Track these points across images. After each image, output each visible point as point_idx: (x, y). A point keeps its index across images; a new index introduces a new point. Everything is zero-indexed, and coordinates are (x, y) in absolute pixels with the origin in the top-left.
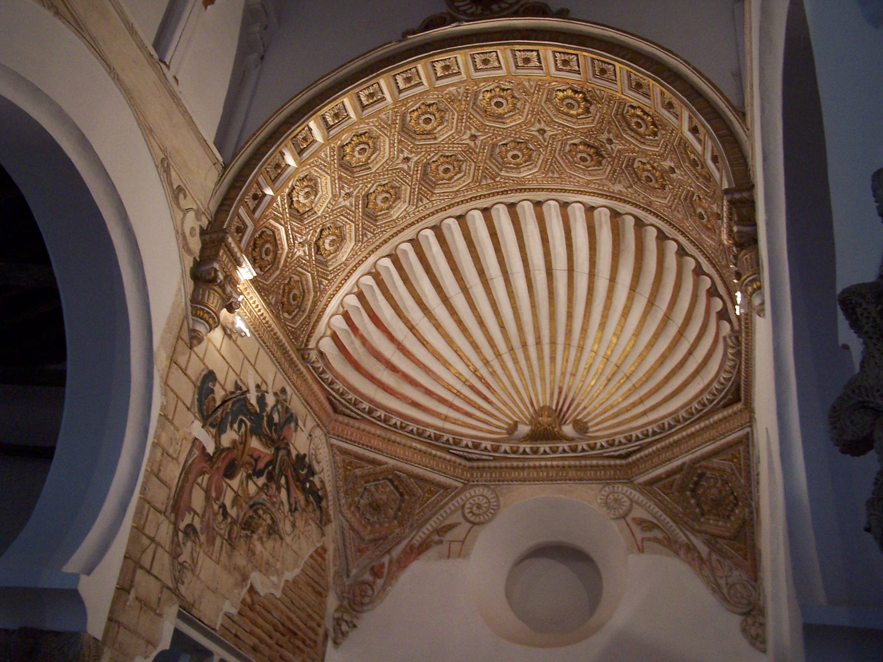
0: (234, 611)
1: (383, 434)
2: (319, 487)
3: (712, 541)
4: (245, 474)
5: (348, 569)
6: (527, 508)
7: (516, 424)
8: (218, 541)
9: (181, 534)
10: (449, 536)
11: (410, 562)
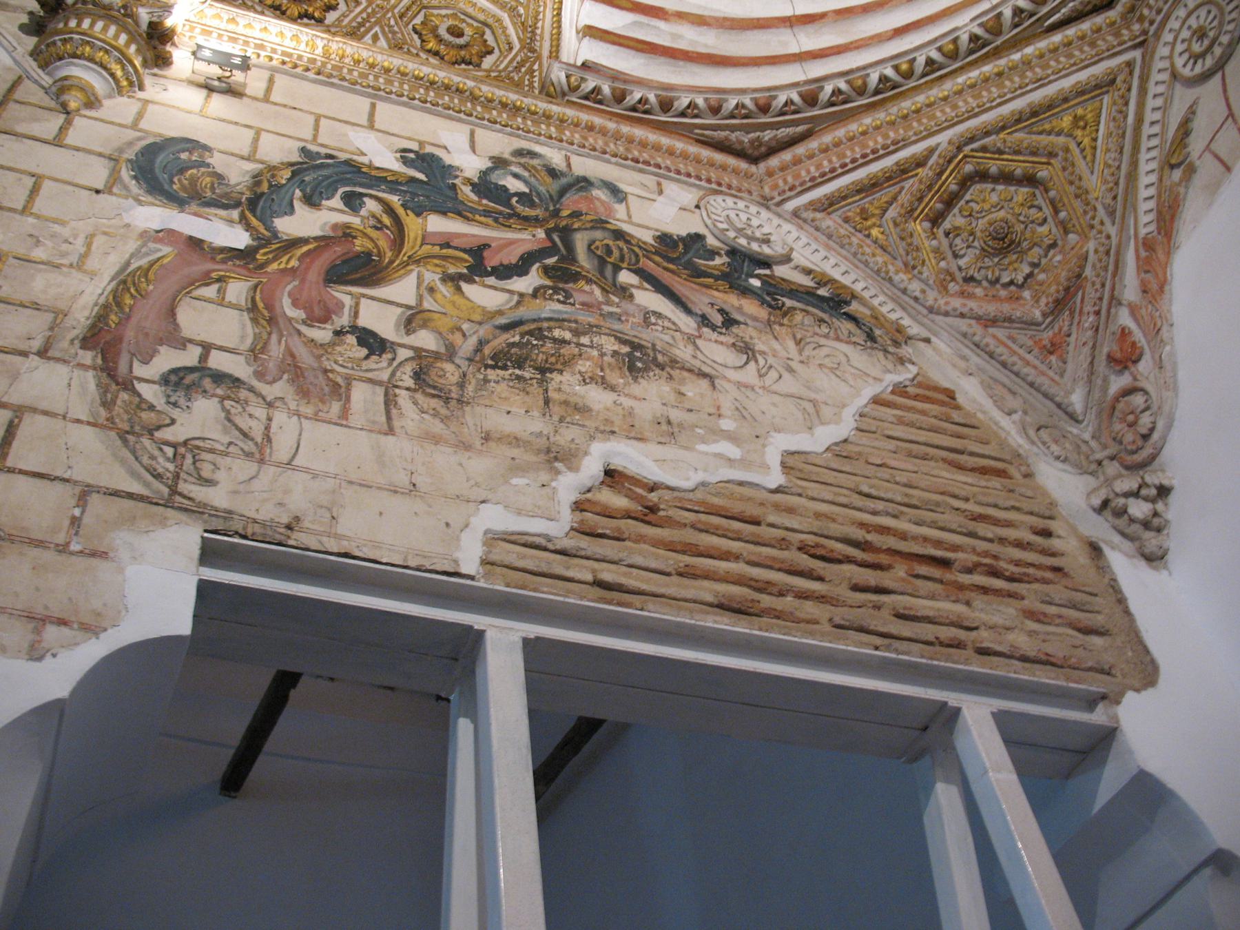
1: (881, 116)
2: (812, 284)
5: (1059, 406)
10: (1196, 145)
11: (1166, 265)
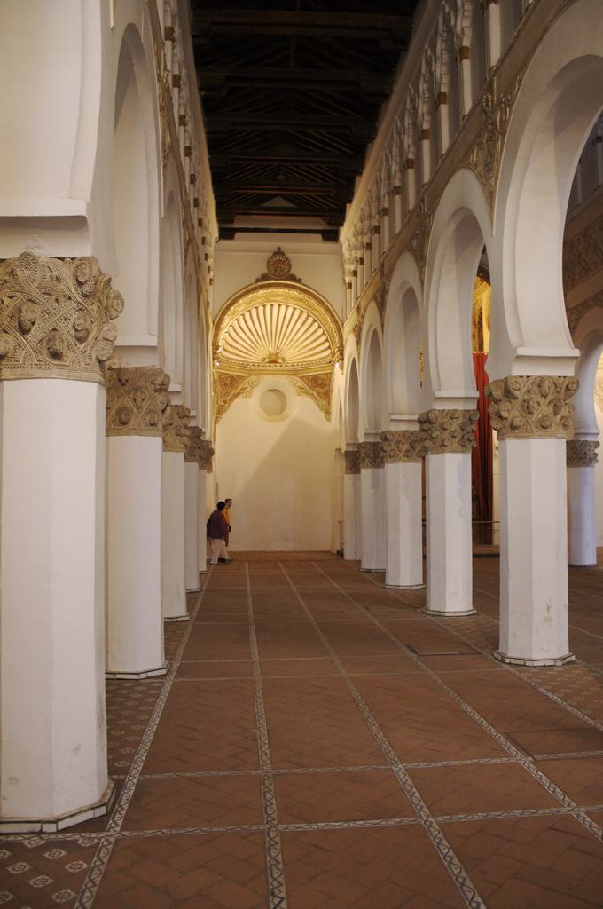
3: (318, 394)
6: (268, 381)
7: (265, 359)
10: (246, 390)
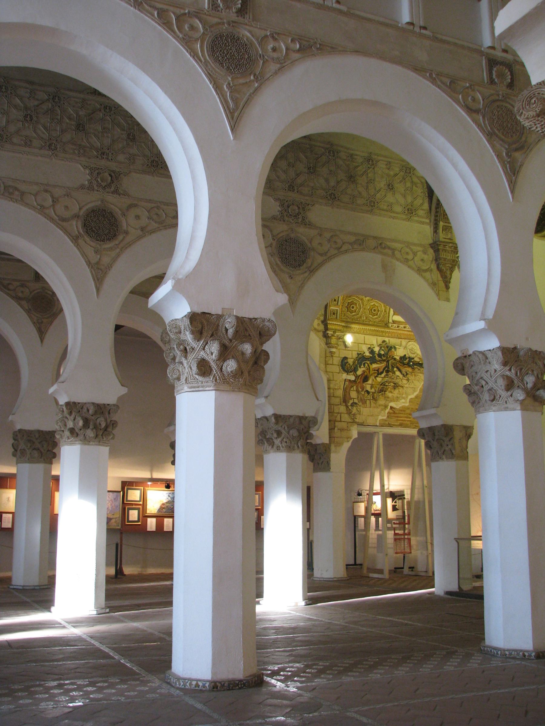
0: (385, 418)
4: (373, 377)
8: (368, 402)
9: (350, 407)
